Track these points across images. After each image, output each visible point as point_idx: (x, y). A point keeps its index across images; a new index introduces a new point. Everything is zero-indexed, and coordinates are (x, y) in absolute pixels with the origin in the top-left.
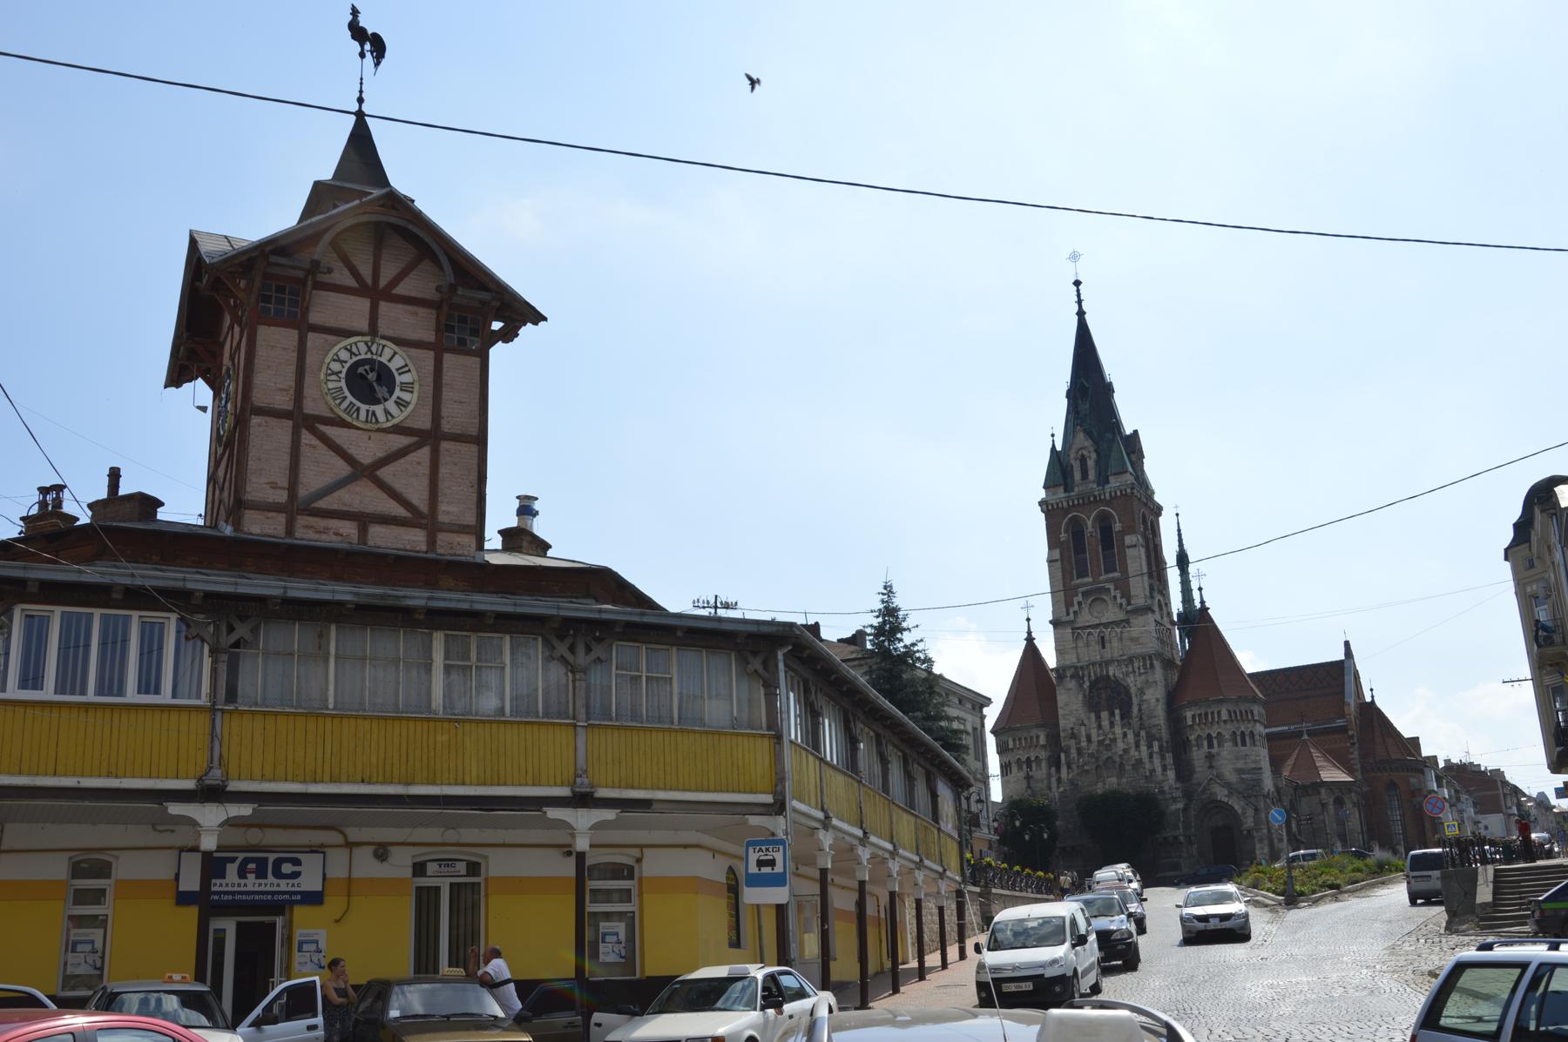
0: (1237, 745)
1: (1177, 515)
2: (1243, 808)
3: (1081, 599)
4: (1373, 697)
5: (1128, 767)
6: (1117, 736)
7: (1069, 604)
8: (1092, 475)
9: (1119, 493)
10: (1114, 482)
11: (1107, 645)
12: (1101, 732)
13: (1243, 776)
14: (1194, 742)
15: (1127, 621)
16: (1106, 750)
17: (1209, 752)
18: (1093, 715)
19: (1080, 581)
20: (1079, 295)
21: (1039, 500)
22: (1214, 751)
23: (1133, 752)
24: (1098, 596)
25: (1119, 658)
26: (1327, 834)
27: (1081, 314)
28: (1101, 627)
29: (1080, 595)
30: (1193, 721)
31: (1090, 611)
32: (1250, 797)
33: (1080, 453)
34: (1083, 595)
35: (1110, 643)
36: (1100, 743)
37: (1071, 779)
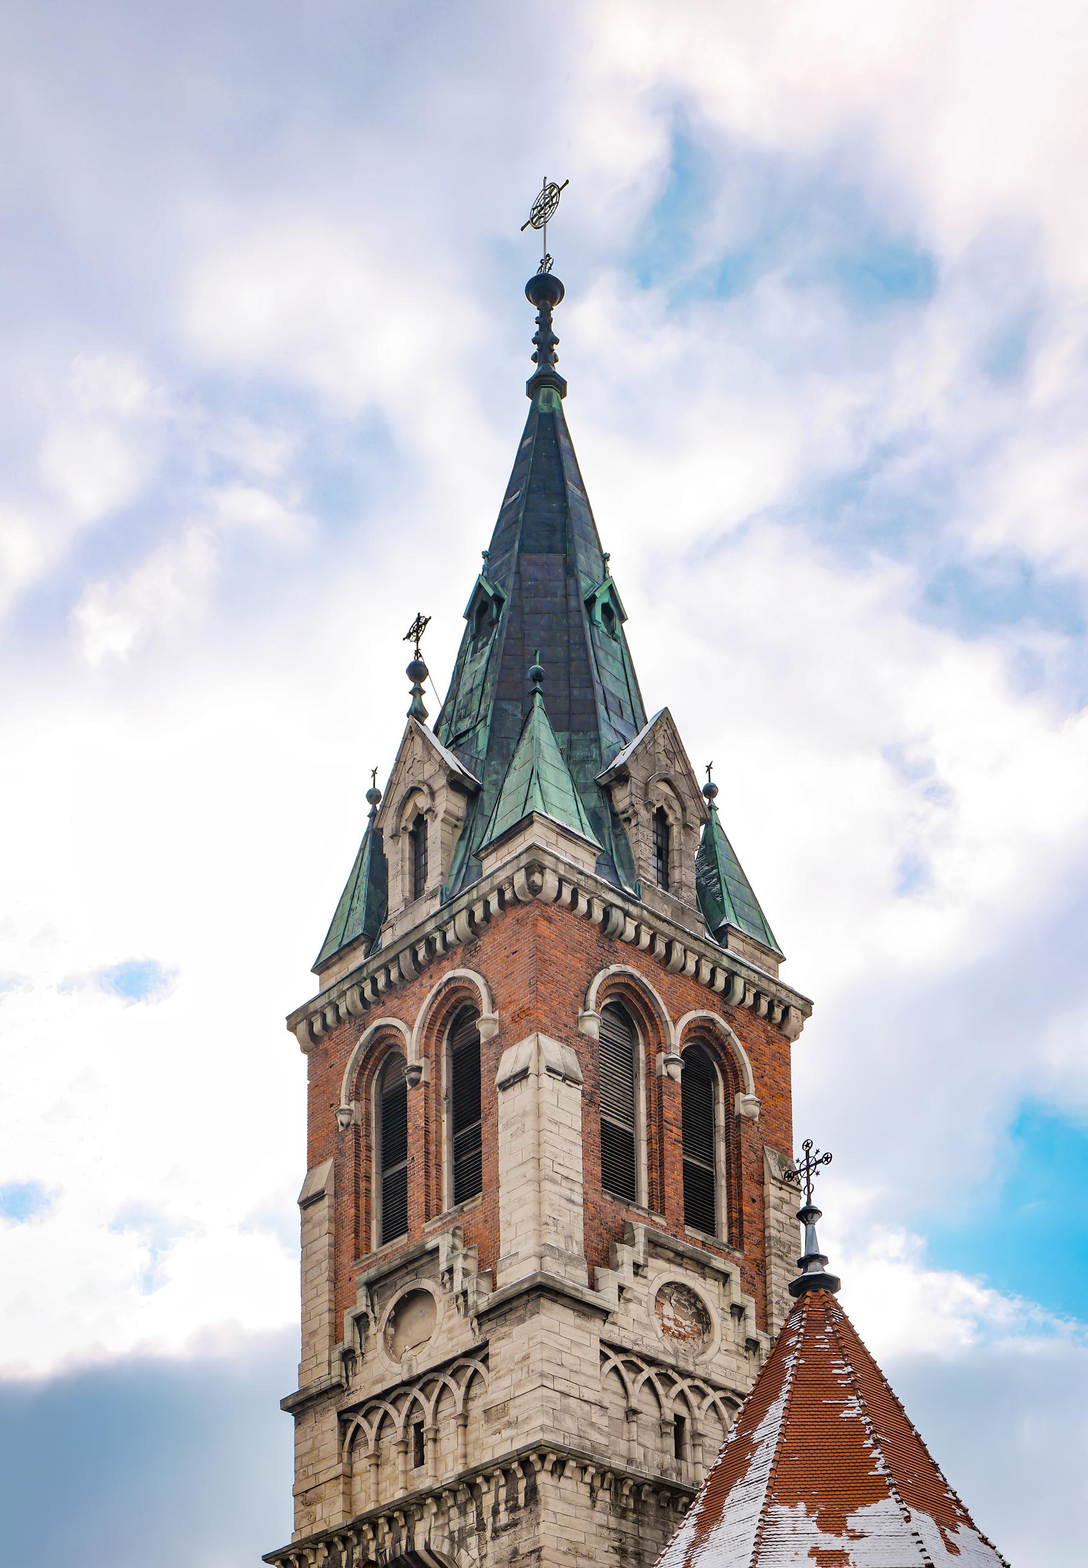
3: (362, 1305)
7: (336, 1337)
15: (480, 1352)
28: (415, 1392)
29: (362, 1293)
35: (435, 1440)
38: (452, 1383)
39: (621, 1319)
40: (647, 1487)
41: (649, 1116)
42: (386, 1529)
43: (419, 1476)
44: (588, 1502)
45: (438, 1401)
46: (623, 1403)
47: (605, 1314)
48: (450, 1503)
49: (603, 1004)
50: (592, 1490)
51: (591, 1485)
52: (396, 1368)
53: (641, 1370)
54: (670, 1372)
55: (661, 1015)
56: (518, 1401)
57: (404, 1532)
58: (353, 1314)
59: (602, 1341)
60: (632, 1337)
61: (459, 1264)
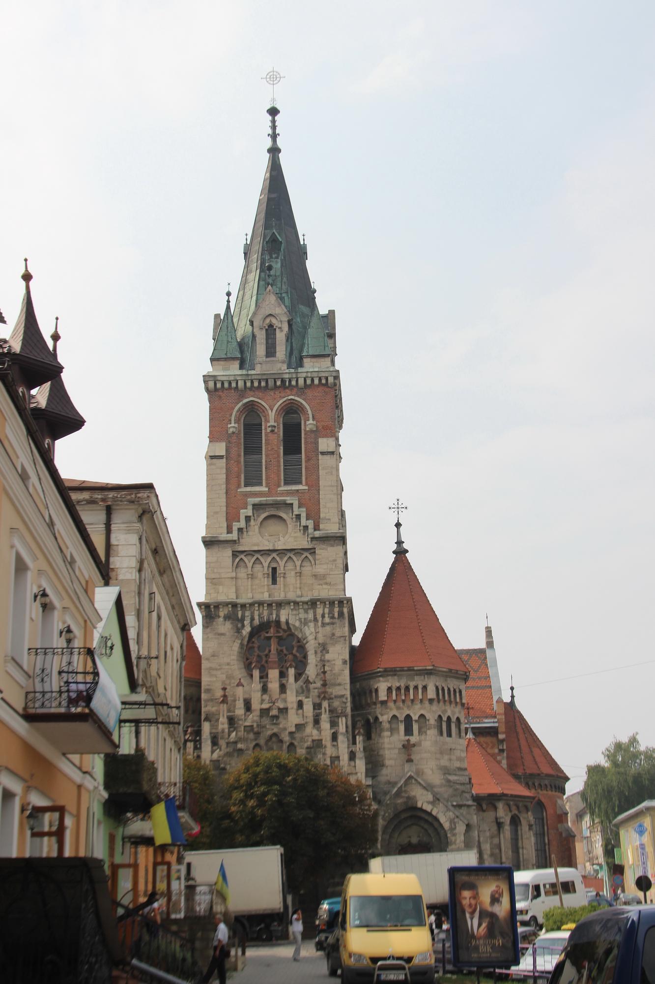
0: (441, 734)
2: (452, 822)
3: (250, 513)
4: (513, 697)
5: (301, 752)
6: (289, 706)
7: (231, 517)
8: (281, 351)
9: (316, 381)
10: (310, 367)
11: (280, 580)
12: (266, 697)
14: (386, 725)
15: (312, 551)
16: (275, 724)
17: (408, 741)
18: (256, 673)
19: (249, 489)
20: (274, 127)
21: (205, 374)
22: (413, 739)
23: (310, 730)
24: (273, 512)
25: (298, 600)
27: (274, 151)
28: (274, 555)
29: (250, 508)
30: (388, 697)
31: (260, 532)
32: (460, 806)
33: (268, 321)
34: (253, 509)
36: (264, 712)
37: (218, 761)
38: (294, 558)
42: (266, 608)
43: (274, 589)
45: (286, 562)
48: (301, 607)
52: (266, 543)
56: (331, 576)
57: (274, 612)
58: (246, 515)
61: (303, 515)
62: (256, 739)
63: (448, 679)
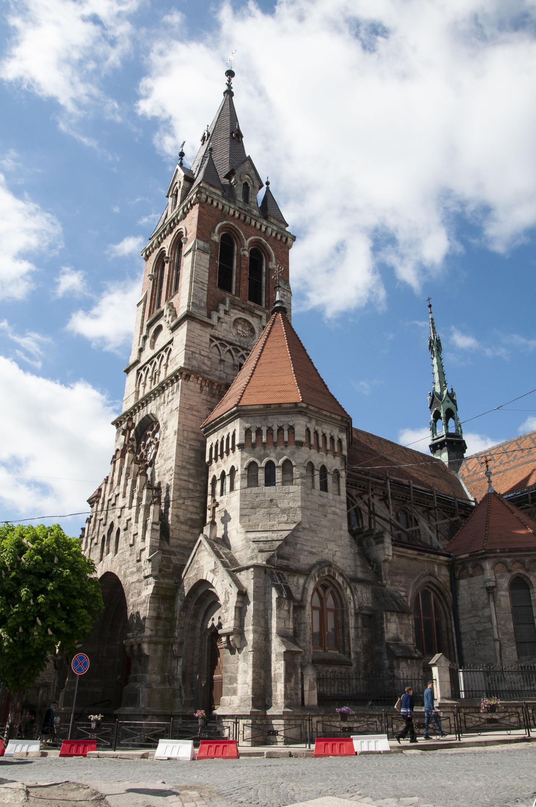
1: (430, 306)
13: (252, 536)
26: (495, 640)
39: (218, 328)
40: (223, 386)
41: (237, 267)
44: (199, 391)
46: (219, 358)
47: (212, 326)
49: (222, 233)
50: (201, 387)
51: (201, 384)
53: (226, 346)
54: (238, 348)
55: (242, 237)
59: (211, 335)
60: (223, 334)
62: (103, 532)
63: (270, 418)
